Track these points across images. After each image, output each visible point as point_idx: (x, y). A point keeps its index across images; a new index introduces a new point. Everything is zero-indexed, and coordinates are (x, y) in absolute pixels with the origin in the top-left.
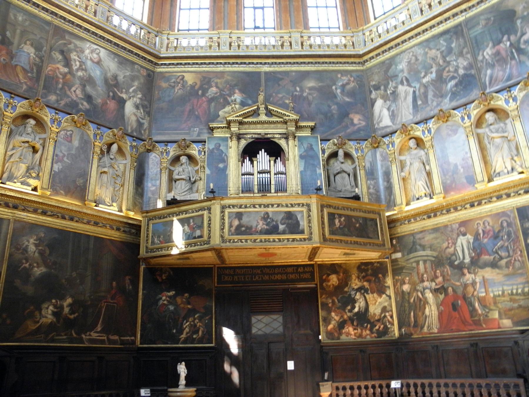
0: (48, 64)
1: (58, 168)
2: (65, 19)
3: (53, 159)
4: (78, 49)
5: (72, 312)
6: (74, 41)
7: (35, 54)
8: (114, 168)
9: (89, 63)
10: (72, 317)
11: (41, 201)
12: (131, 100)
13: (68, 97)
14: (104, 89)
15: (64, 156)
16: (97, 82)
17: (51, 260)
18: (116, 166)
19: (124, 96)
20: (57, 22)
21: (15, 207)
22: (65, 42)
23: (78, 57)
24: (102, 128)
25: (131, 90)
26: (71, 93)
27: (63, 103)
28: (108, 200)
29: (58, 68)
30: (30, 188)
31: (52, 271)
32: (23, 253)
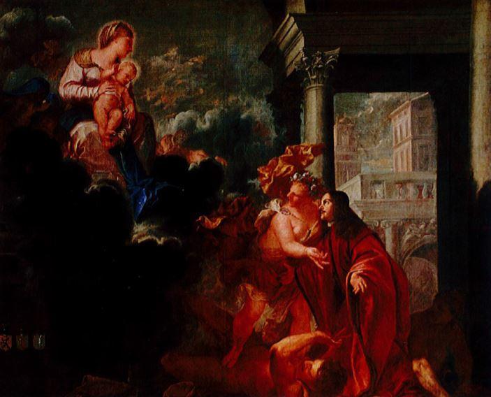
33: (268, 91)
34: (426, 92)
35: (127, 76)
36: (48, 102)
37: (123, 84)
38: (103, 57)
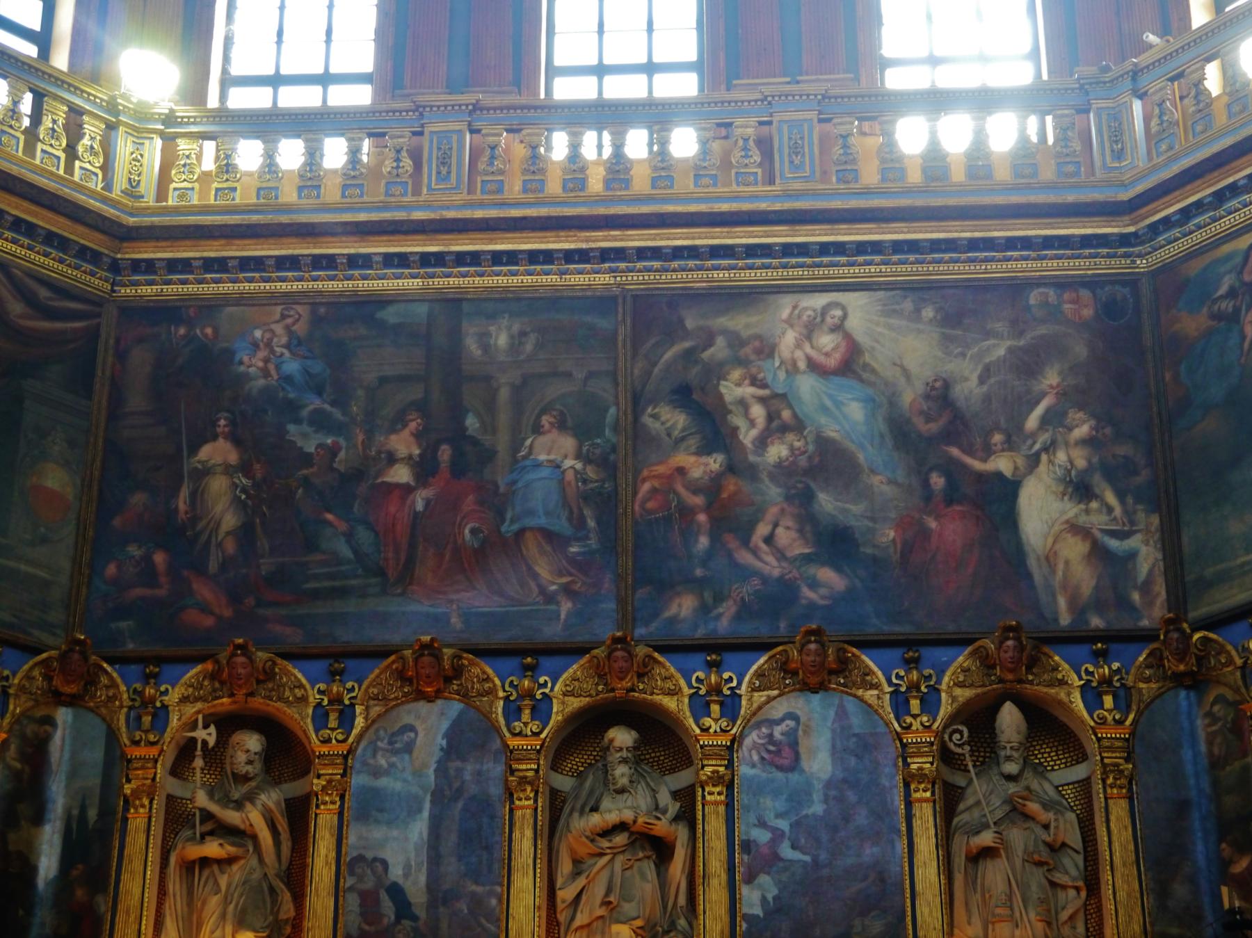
0: (637, 473)
1: (764, 899)
2: (656, 253)
3: (731, 869)
4: (747, 350)
6: (723, 322)
7: (578, 456)
8: (1027, 817)
9: (807, 387)
12: (1043, 468)
13: (745, 573)
14: (901, 475)
15: (778, 835)
16: (861, 457)
18: (1033, 807)
19: (1003, 464)
20: (637, 278)
22: (687, 344)
23: (754, 382)
24: (928, 653)
25: (1032, 422)
26: (755, 552)
27: (727, 610)
29: (681, 471)
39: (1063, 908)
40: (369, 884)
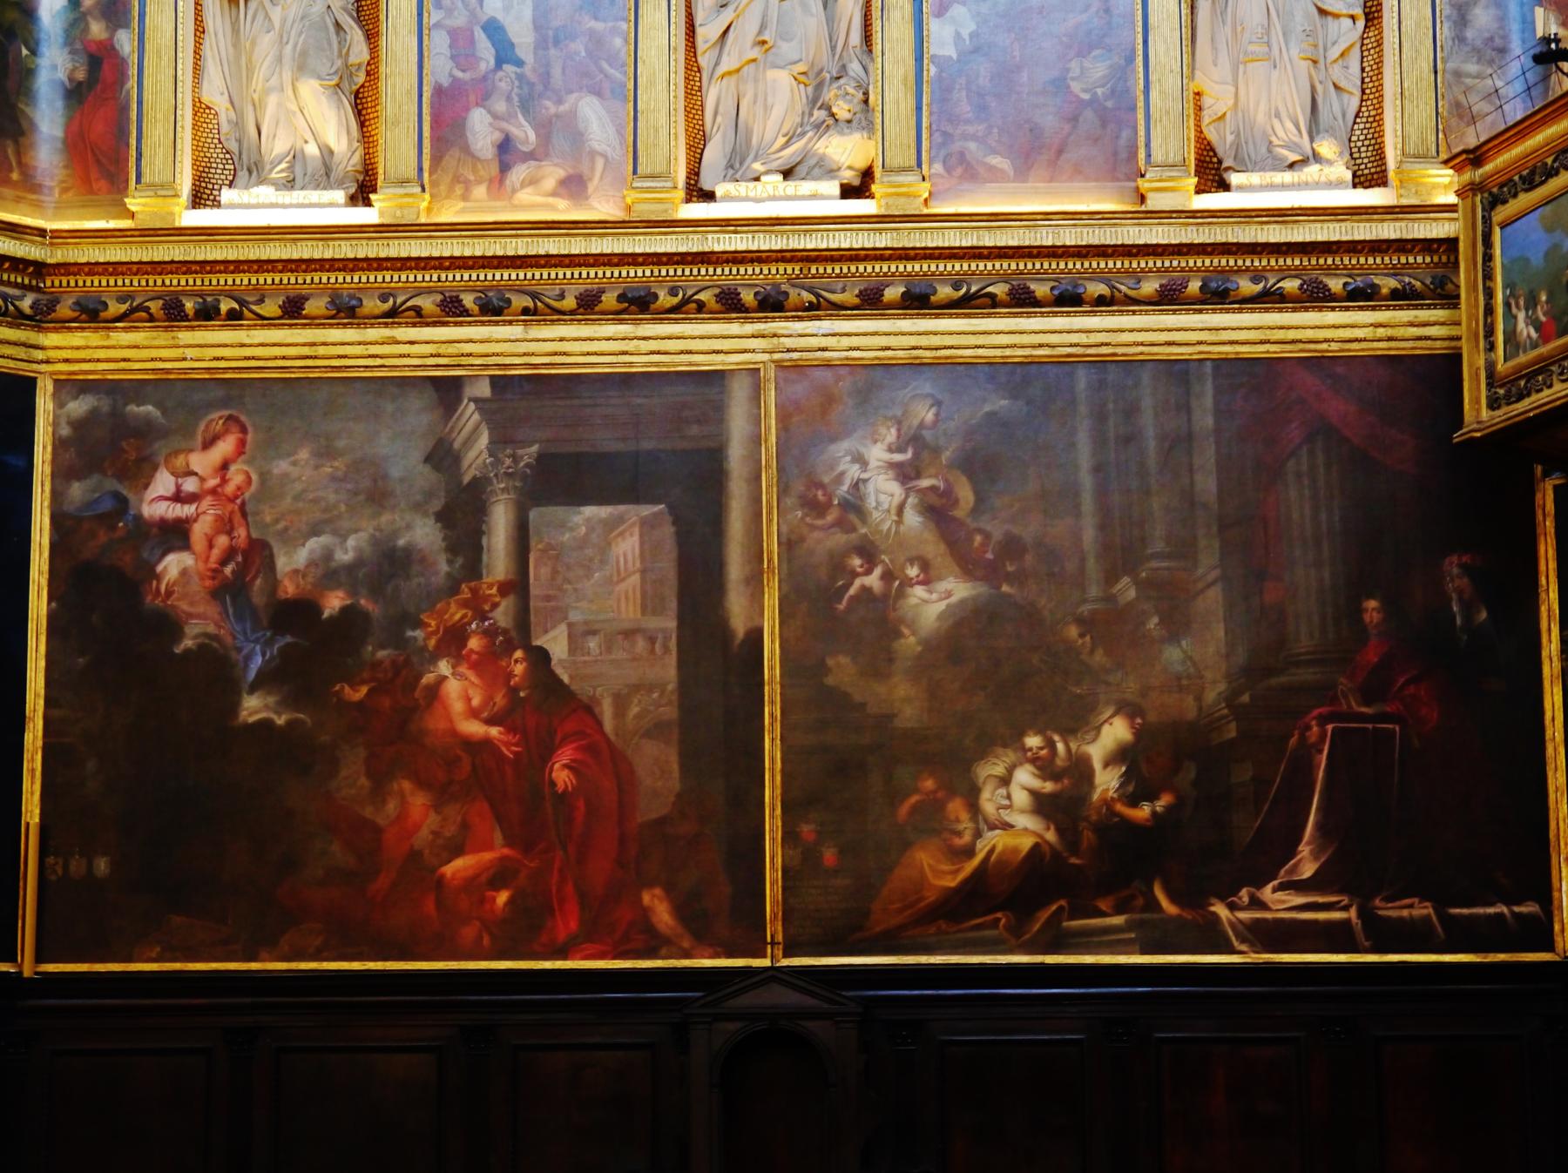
1: (958, 35)
5: (1138, 787)
10: (1143, 812)
11: (882, 241)
17: (987, 536)
21: (772, 304)
28: (1287, 134)
30: (833, 188)
31: (1005, 588)
32: (842, 524)
33: (437, 505)
34: (661, 503)
35: (239, 488)
36: (126, 525)
37: (232, 500)
38: (202, 462)
39: (1334, 44)
40: (459, 20)
